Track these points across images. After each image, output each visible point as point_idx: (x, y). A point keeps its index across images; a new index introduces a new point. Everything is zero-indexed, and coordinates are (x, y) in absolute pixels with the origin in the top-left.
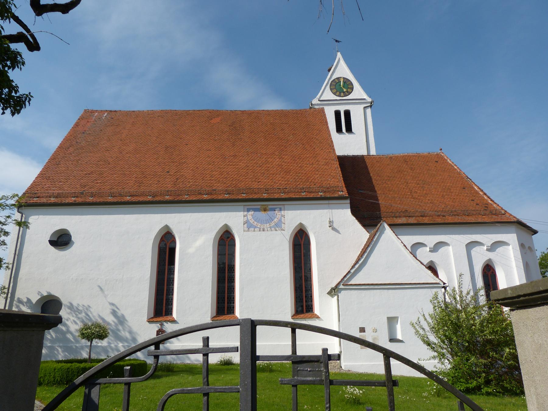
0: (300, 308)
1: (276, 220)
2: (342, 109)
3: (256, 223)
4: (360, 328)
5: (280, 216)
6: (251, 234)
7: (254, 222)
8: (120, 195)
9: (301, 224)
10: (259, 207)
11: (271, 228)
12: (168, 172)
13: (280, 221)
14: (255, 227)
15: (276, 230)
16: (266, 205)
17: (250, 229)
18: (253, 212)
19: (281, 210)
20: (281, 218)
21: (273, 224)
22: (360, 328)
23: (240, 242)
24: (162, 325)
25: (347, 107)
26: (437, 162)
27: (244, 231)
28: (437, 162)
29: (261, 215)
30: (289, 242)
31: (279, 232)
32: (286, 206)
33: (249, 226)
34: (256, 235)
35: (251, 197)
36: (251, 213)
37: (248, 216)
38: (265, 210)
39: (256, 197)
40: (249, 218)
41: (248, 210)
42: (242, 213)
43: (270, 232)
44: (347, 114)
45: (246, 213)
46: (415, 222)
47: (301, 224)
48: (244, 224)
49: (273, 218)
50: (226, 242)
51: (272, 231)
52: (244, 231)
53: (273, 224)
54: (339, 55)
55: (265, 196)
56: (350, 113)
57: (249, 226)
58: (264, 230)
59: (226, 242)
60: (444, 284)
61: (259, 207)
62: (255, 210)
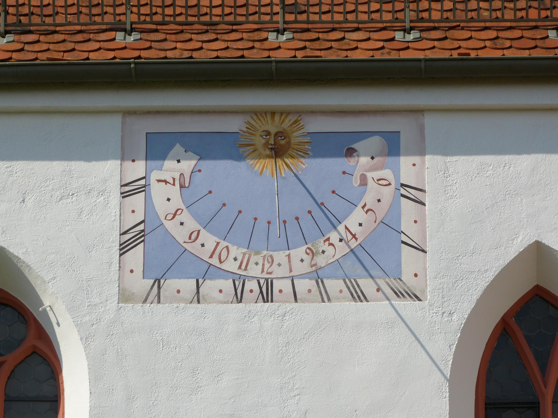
1: (355, 220)
3: (209, 239)
5: (387, 193)
6: (173, 317)
7: (193, 237)
10: (234, 125)
11: (317, 276)
13: (389, 225)
14: (209, 271)
15: (359, 296)
16: (285, 113)
18: (187, 165)
19: (392, 147)
20: (394, 210)
21: (333, 252)
23: (95, 377)
27: (125, 297)
29: (250, 180)
30: (454, 382)
31: (378, 309)
32: (430, 122)
33: (156, 258)
34: (208, 326)
35: (176, 50)
36: (171, 168)
37: (158, 192)
38: (279, 149)
39: (210, 50)
40: (162, 208)
41: (157, 149)
42: (108, 172)
43: (311, 311)
45: (138, 169)
48: (124, 248)
49: (332, 203)
51: (325, 297)
52: (125, 297)
55: (282, 45)
57: (156, 258)
58: (267, 294)
61: (234, 125)
62: (204, 147)
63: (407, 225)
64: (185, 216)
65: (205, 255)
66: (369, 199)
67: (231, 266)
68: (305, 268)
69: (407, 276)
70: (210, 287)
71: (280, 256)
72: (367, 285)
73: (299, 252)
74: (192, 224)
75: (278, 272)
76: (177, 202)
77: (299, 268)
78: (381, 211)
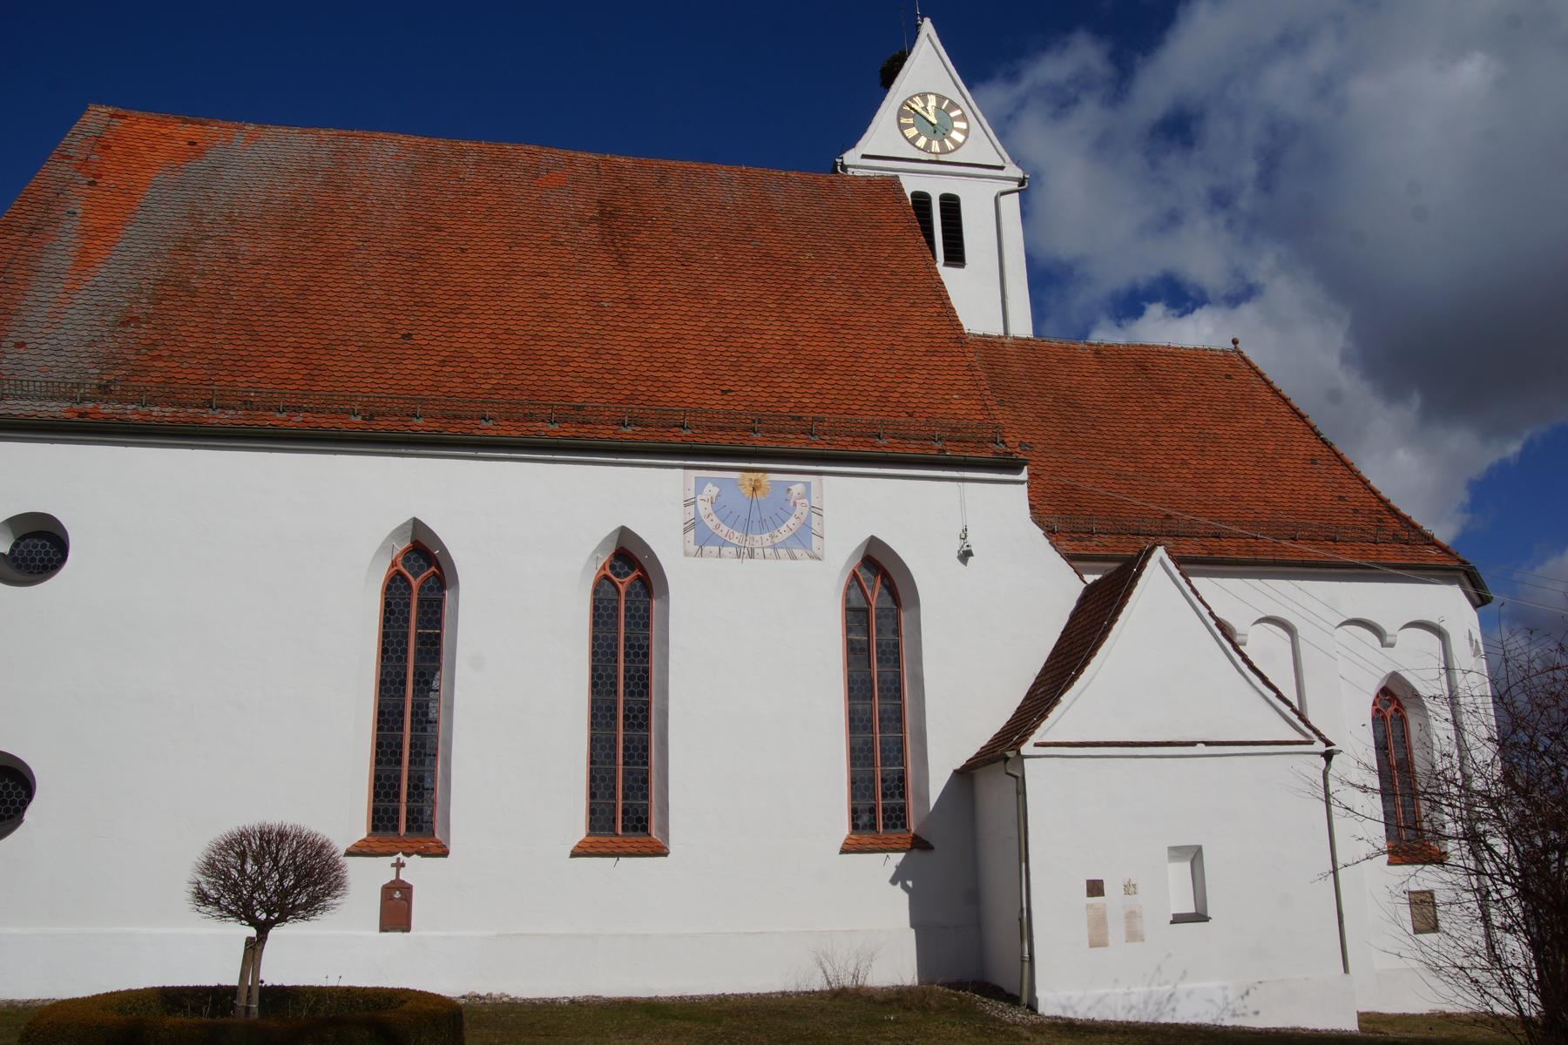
0: (865, 818)
1: (792, 521)
3: (725, 528)
4: (1089, 882)
7: (717, 527)
8: (247, 405)
9: (873, 542)
11: (774, 547)
12: (409, 336)
13: (807, 525)
14: (724, 543)
15: (793, 557)
17: (706, 549)
20: (809, 518)
22: (1089, 882)
24: (399, 865)
26: (1228, 377)
27: (686, 554)
28: (1228, 377)
33: (702, 537)
34: (725, 568)
37: (700, 505)
40: (702, 512)
44: (951, 206)
46: (1204, 554)
47: (873, 542)
48: (686, 531)
50: (628, 589)
52: (686, 554)
53: (784, 532)
54: (927, 27)
57: (702, 537)
59: (628, 589)
60: (1328, 744)
63: (815, 525)
64: (714, 517)
65: (722, 535)
66: (797, 512)
67: (735, 541)
68: (769, 543)
69: (815, 548)
70: (725, 550)
71: (757, 537)
72: (797, 552)
73: (766, 536)
74: (716, 521)
75: (756, 545)
76: (710, 510)
77: (767, 543)
78: (803, 518)
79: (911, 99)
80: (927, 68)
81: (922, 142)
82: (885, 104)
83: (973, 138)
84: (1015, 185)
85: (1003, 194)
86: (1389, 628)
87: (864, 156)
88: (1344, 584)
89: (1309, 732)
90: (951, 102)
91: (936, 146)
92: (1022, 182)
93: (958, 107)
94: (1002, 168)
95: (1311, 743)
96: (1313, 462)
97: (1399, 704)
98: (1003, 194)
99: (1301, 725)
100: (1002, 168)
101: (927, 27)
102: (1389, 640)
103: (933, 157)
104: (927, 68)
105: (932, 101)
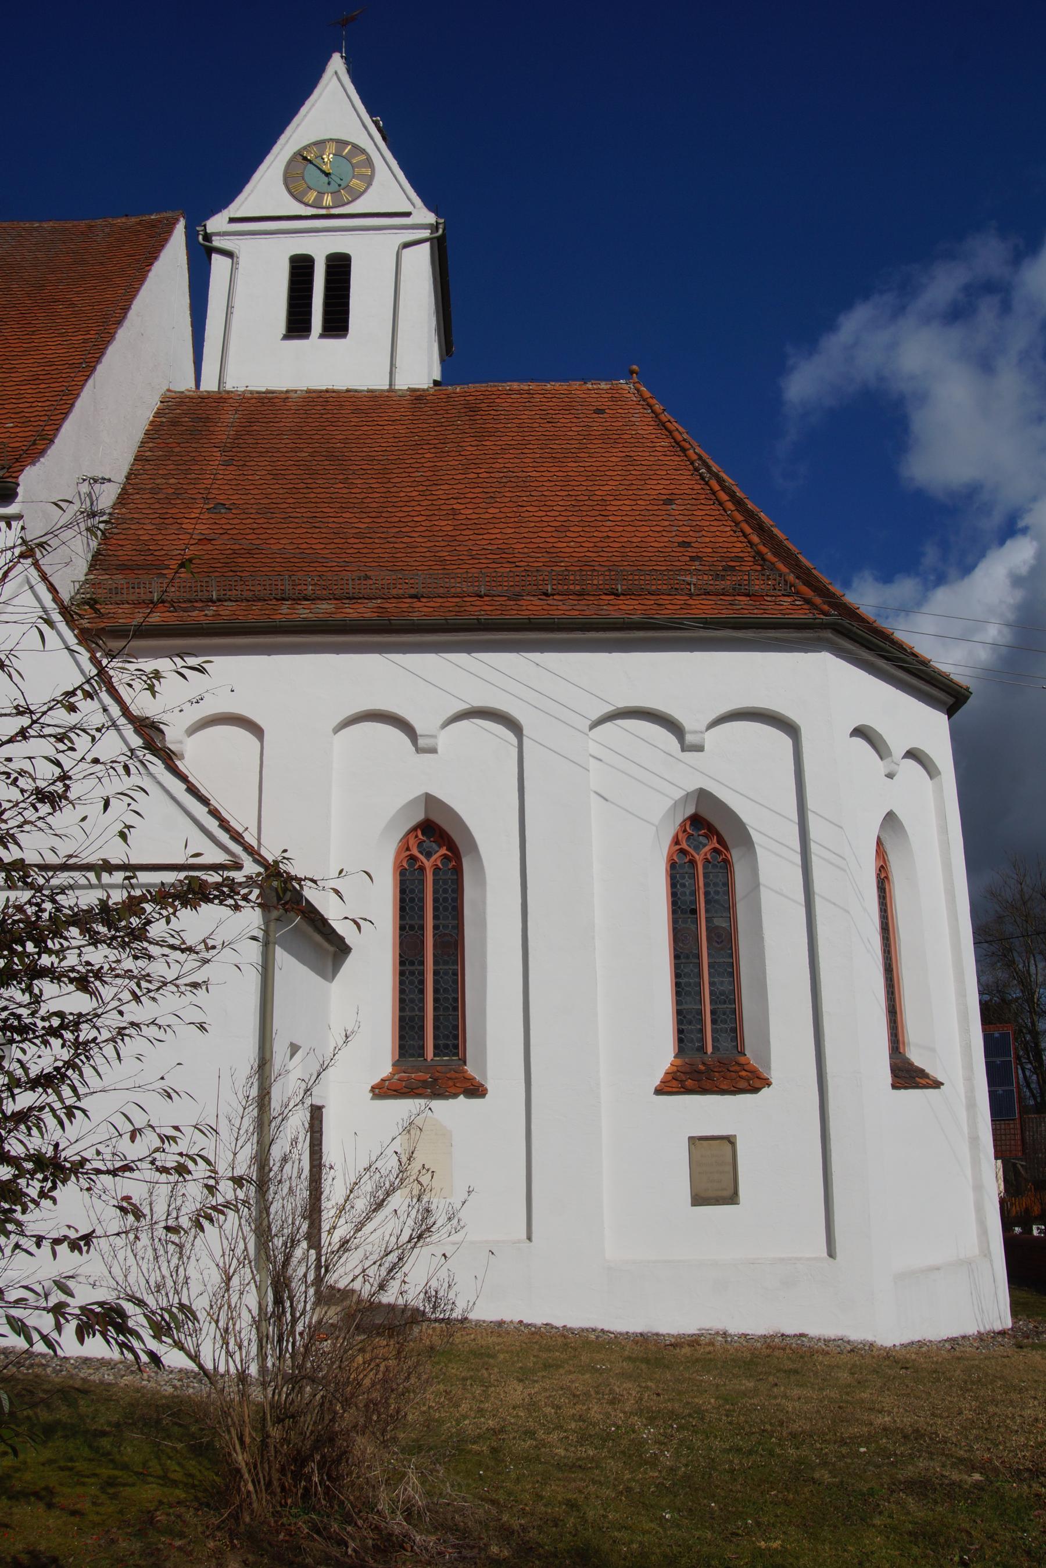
2: (319, 249)
25: (339, 244)
44: (340, 268)
56: (349, 266)
79: (305, 148)
80: (333, 110)
81: (312, 196)
82: (269, 159)
83: (389, 187)
84: (426, 234)
85: (407, 245)
86: (692, 722)
87: (232, 220)
88: (616, 656)
89: (237, 849)
90: (355, 147)
91: (328, 200)
92: (434, 228)
93: (363, 151)
94: (408, 214)
95: (238, 867)
96: (669, 502)
97: (721, 841)
98: (407, 245)
99: (224, 837)
100: (408, 214)
101: (337, 63)
102: (689, 738)
103: (323, 212)
104: (333, 110)
105: (331, 148)
